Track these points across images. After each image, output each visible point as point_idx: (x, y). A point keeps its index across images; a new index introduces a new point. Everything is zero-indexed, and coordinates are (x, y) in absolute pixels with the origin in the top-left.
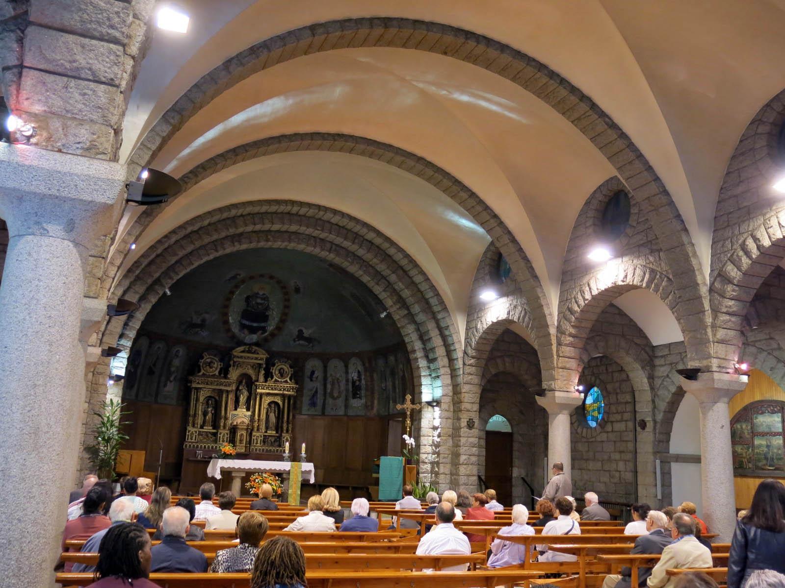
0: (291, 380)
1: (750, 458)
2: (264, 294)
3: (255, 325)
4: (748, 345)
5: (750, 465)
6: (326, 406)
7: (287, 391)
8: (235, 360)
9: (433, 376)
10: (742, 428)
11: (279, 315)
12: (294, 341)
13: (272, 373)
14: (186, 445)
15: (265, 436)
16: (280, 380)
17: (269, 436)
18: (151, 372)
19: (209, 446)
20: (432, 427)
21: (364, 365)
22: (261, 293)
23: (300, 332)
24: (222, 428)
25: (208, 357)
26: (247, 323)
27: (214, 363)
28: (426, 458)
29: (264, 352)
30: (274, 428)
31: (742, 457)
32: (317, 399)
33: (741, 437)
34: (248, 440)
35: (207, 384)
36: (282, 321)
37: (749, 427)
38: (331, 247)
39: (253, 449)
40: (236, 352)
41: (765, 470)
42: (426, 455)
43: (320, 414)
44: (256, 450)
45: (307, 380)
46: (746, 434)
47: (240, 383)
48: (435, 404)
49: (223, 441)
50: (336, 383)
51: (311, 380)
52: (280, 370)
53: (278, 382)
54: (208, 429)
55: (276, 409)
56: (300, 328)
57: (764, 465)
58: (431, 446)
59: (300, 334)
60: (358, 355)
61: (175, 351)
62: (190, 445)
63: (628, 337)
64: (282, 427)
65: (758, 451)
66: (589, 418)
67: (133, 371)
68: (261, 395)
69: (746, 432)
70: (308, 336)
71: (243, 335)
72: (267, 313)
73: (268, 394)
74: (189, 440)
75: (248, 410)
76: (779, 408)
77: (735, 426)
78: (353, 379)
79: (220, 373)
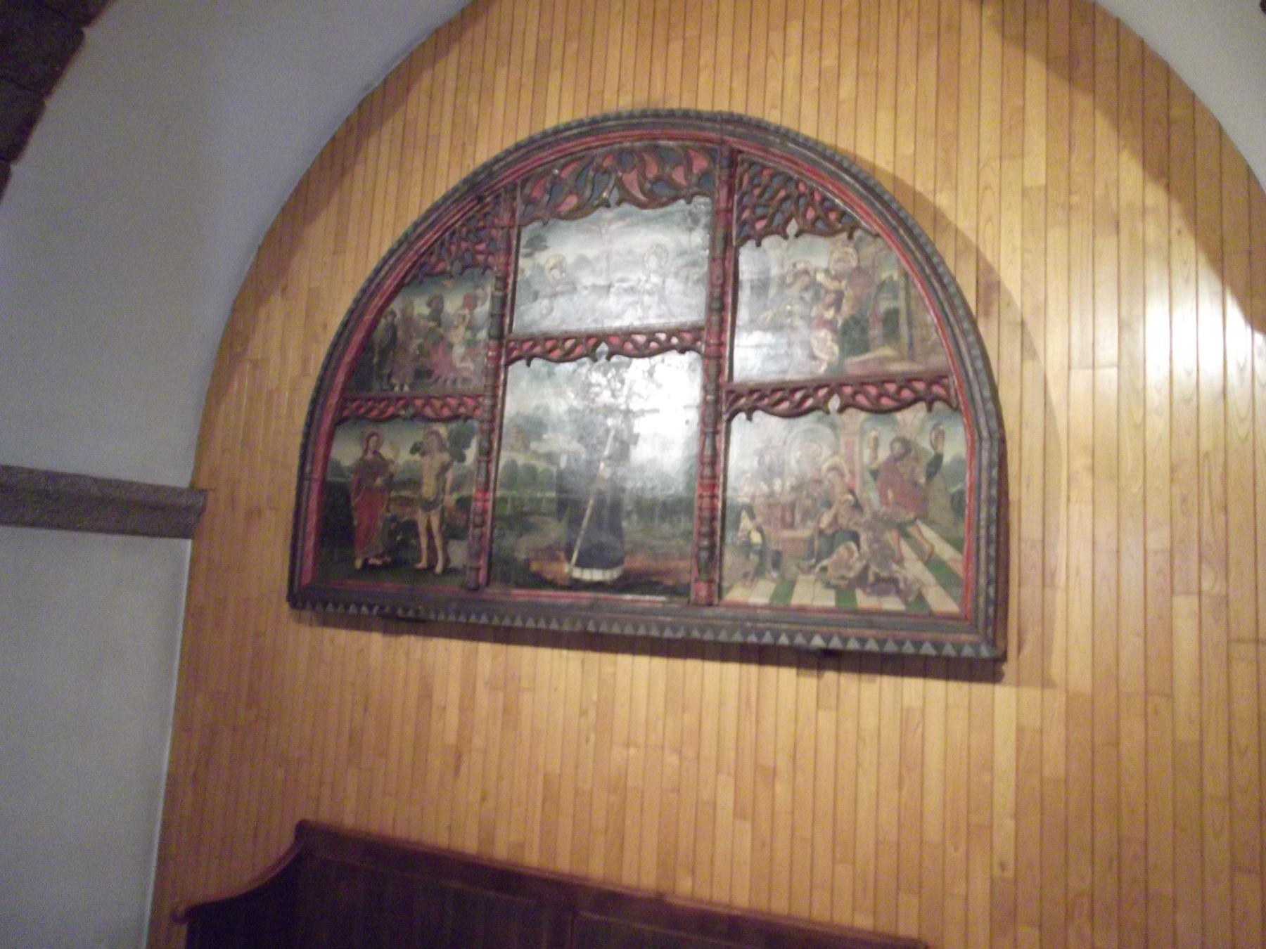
1: (464, 503)
5: (459, 554)
10: (437, 314)
31: (408, 502)
33: (423, 374)
41: (552, 584)
46: (459, 350)
57: (551, 553)
65: (521, 460)
69: (458, 336)
76: (700, 163)
77: (396, 305)
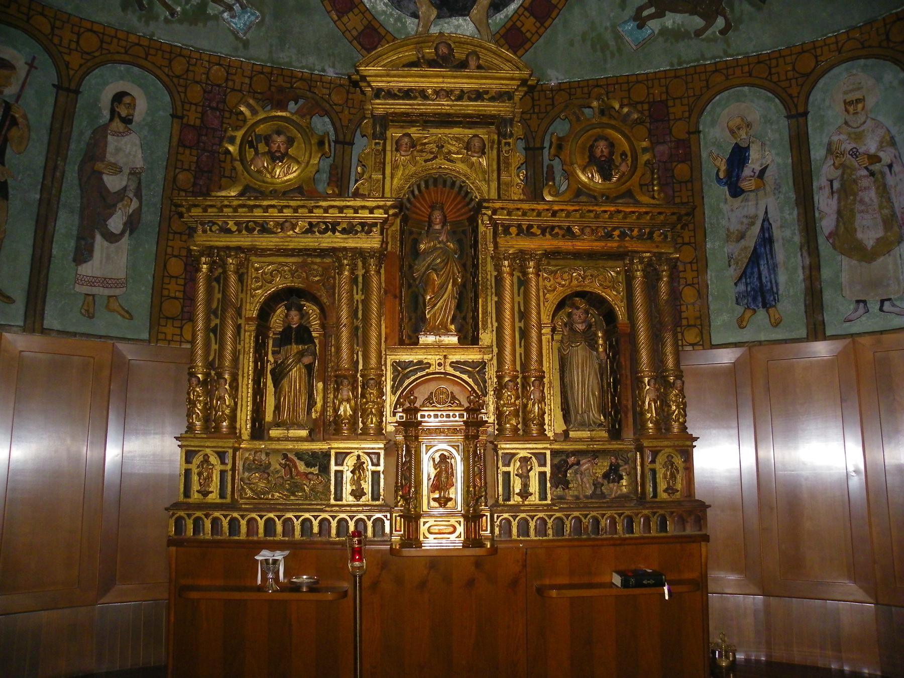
6: (828, 295)
7: (640, 237)
8: (381, 107)
12: (641, 23)
17: (575, 453)
19: (287, 522)
25: (262, 116)
27: (290, 141)
32: (773, 269)
35: (265, 230)
43: (803, 333)
49: (358, 493)
50: (866, 182)
51: (736, 191)
62: (197, 523)
71: (411, 24)
74: (195, 497)
75: (469, 338)
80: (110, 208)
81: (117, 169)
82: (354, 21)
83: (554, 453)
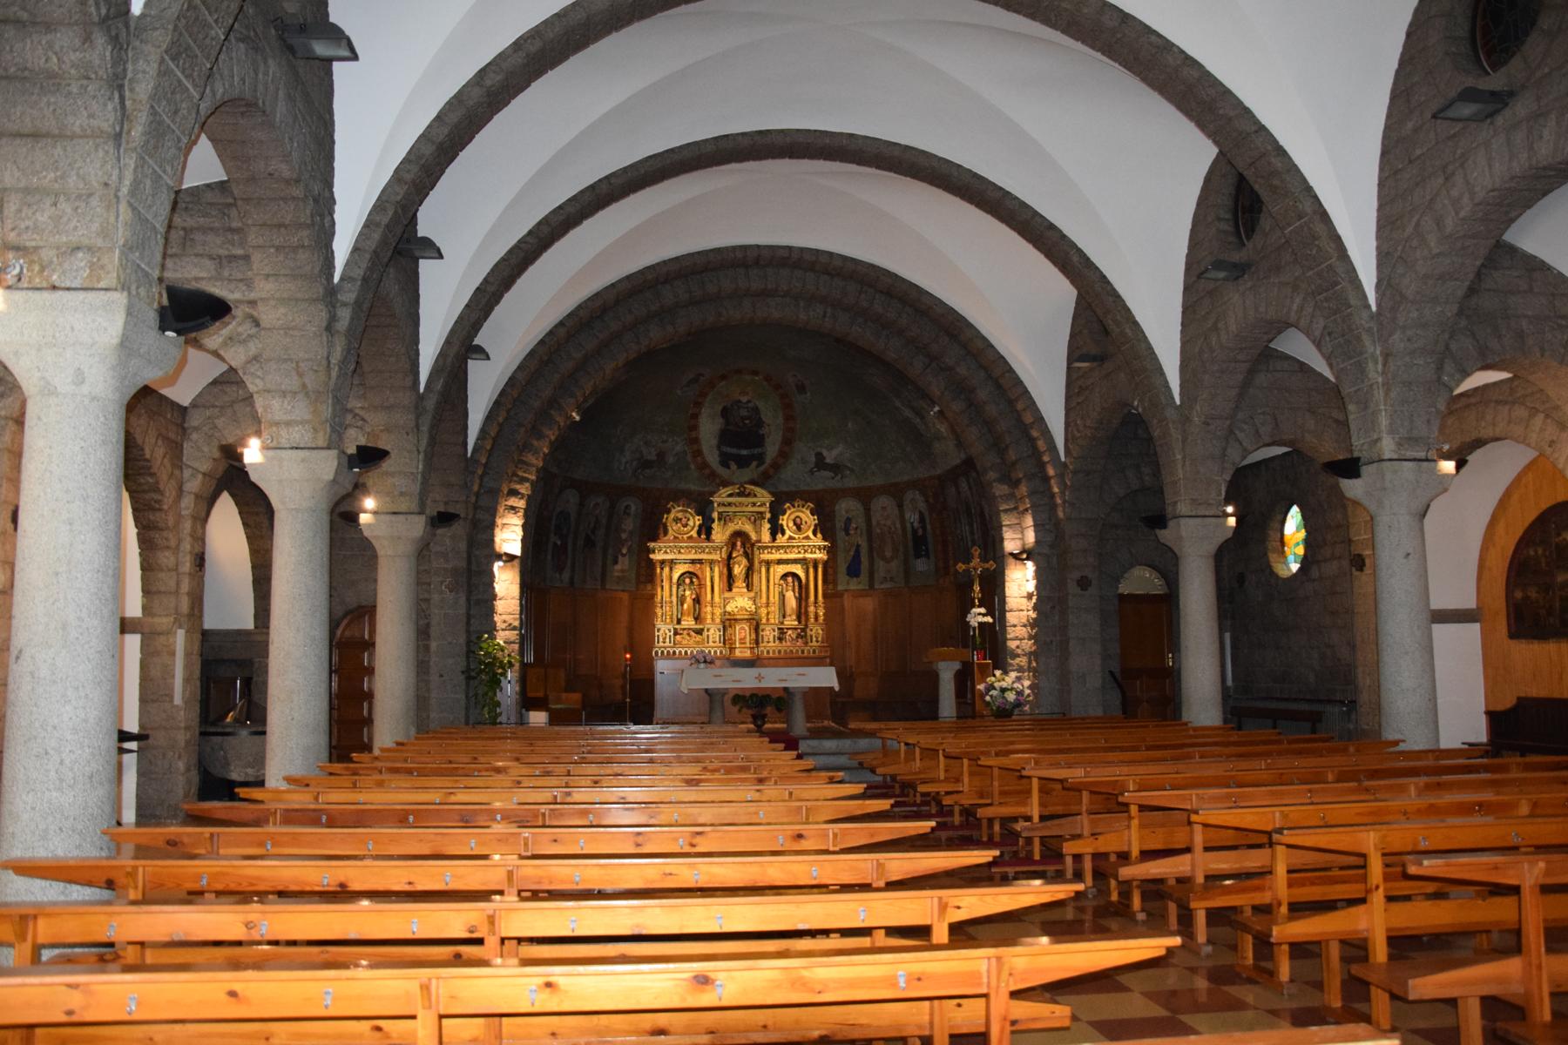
0: (815, 534)
2: (749, 401)
3: (744, 452)
4: (1514, 403)
7: (811, 553)
9: (1021, 509)
11: (781, 433)
12: (812, 472)
13: (782, 525)
14: (657, 653)
15: (782, 629)
16: (796, 536)
18: (590, 543)
20: (1025, 594)
21: (927, 501)
22: (744, 399)
23: (819, 456)
24: (709, 621)
26: (734, 451)
28: (1018, 647)
29: (765, 492)
30: (794, 617)
34: (753, 636)
36: (787, 442)
37: (1547, 553)
38: (825, 313)
39: (762, 652)
40: (719, 496)
42: (1018, 642)
44: (768, 652)
45: (841, 535)
47: (731, 545)
48: (1025, 556)
51: (848, 534)
52: (794, 521)
53: (794, 539)
54: (688, 622)
55: (796, 584)
56: (819, 450)
58: (1025, 626)
59: (821, 463)
60: (914, 484)
61: (623, 508)
62: (662, 652)
63: (1320, 411)
64: (807, 613)
66: (1291, 558)
67: (559, 543)
68: (768, 563)
70: (832, 462)
72: (761, 432)
73: (780, 562)
74: (661, 644)
78: (913, 527)
79: (699, 533)
80: (623, 545)
81: (625, 531)
82: (707, 471)
83: (779, 629)
